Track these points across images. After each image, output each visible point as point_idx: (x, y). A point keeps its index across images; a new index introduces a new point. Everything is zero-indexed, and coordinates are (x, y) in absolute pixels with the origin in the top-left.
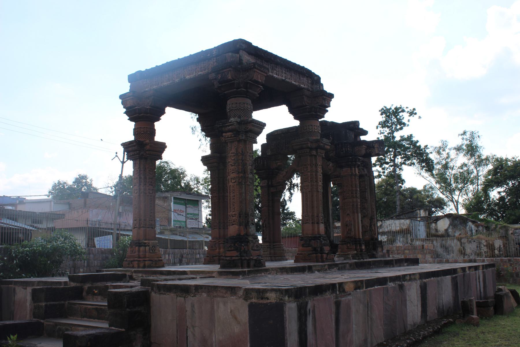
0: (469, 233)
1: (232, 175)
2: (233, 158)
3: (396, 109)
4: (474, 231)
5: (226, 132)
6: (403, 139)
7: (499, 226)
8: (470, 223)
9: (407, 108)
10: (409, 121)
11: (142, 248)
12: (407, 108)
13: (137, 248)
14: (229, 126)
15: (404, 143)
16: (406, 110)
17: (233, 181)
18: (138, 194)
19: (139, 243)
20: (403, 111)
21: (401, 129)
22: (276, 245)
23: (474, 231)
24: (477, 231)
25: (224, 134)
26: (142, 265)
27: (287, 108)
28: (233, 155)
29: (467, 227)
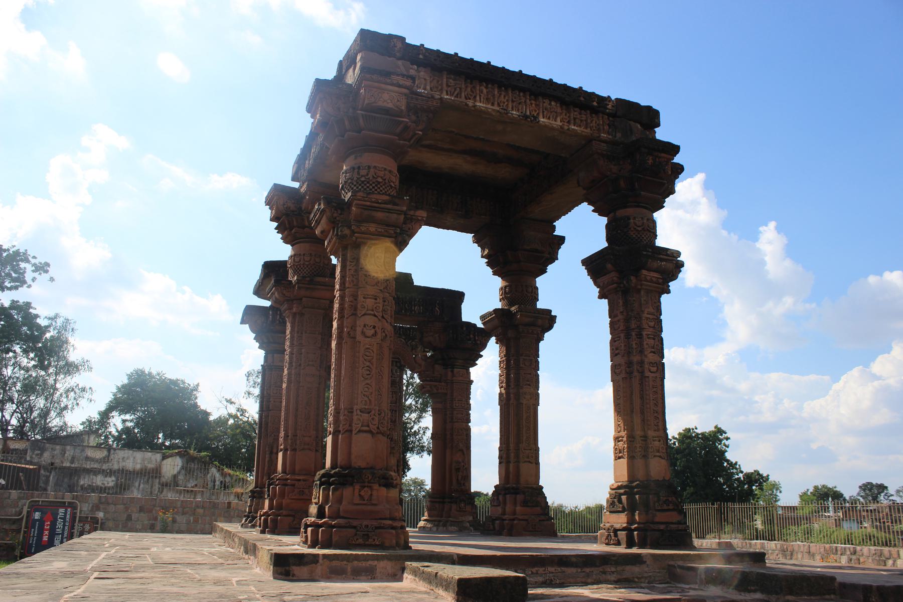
0: (210, 485)
3: (17, 253)
4: (218, 483)
5: (649, 270)
6: (14, 305)
8: (213, 470)
9: (34, 257)
10: (34, 280)
12: (34, 257)
13: (384, 490)
14: (662, 260)
15: (14, 312)
16: (33, 261)
20: (28, 261)
21: (16, 288)
23: (218, 483)
25: (644, 272)
27: (465, 240)
29: (209, 475)
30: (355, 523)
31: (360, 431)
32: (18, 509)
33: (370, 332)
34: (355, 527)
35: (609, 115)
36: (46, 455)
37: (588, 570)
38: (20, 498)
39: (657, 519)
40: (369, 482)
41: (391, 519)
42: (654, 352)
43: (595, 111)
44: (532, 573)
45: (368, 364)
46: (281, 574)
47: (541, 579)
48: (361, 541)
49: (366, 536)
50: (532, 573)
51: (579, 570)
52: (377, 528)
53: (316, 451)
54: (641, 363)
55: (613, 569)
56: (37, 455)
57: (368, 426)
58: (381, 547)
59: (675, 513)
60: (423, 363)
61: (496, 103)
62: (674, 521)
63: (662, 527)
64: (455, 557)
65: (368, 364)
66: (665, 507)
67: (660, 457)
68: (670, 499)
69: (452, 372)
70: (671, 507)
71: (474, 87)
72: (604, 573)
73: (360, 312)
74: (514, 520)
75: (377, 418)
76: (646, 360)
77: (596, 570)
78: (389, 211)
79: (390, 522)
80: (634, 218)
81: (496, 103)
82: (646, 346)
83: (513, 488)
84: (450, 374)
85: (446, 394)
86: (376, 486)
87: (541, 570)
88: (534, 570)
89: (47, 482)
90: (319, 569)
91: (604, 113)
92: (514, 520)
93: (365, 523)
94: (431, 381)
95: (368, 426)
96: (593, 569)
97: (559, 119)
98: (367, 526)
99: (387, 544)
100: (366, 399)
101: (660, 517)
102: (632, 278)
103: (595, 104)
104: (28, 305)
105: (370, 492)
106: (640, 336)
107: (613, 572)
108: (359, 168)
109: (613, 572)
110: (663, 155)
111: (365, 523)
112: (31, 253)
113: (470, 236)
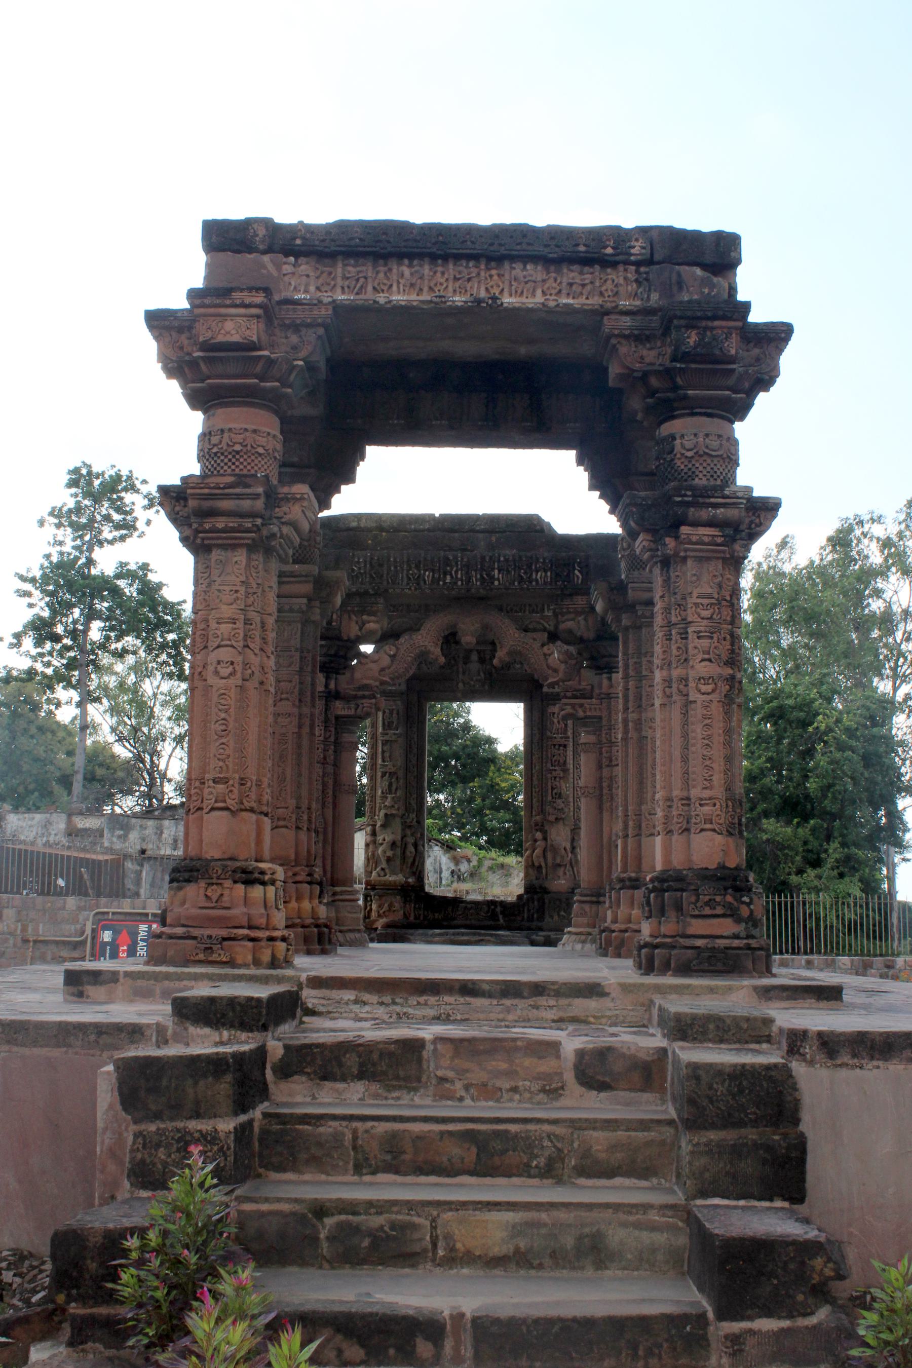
1: (703, 669)
2: (706, 613)
3: (117, 478)
5: (695, 524)
6: (124, 572)
7: (487, 863)
9: (144, 482)
10: (148, 523)
11: (257, 891)
12: (144, 482)
13: (241, 887)
14: (715, 506)
15: (122, 583)
17: (704, 688)
18: (237, 680)
19: (244, 871)
21: (123, 538)
22: (342, 893)
24: (453, 872)
25: (685, 530)
26: (266, 957)
28: (705, 601)
30: (195, 932)
31: (213, 809)
32: (78, 926)
33: (225, 672)
34: (195, 938)
35: (638, 264)
36: (133, 836)
37: (508, 1002)
38: (80, 909)
39: (691, 931)
40: (218, 878)
41: (250, 927)
42: (710, 660)
43: (607, 263)
44: (419, 1003)
45: (223, 715)
46: (73, 994)
47: (431, 1012)
48: (201, 956)
49: (209, 950)
50: (419, 1003)
51: (495, 1002)
52: (224, 939)
53: (298, 828)
54: (684, 680)
55: (552, 1002)
56: (119, 837)
57: (225, 801)
58: (231, 963)
59: (729, 921)
61: (426, 289)
62: (725, 934)
63: (699, 943)
64: (457, 986)
65: (223, 715)
66: (707, 911)
67: (714, 830)
68: (718, 898)
69: (610, 679)
70: (719, 910)
71: (390, 270)
72: (537, 1007)
73: (213, 643)
74: (626, 931)
75: (236, 791)
76: (692, 674)
77: (521, 1003)
78: (239, 497)
79: (245, 932)
80: (682, 436)
81: (426, 289)
82: (691, 651)
83: (630, 879)
84: (605, 682)
85: (600, 718)
86: (228, 883)
87: (432, 1000)
88: (422, 999)
89: (138, 882)
90: (120, 989)
91: (627, 263)
92: (626, 931)
93: (208, 932)
94: (576, 697)
95: (225, 801)
96: (516, 1001)
97: (539, 292)
98: (210, 937)
99: (239, 961)
100: (221, 764)
101: (697, 926)
102: (668, 540)
103: (609, 251)
104: (145, 567)
105: (219, 892)
106: (684, 636)
107: (551, 1007)
108: (210, 433)
109: (551, 1007)
110: (717, 323)
111: (208, 932)
112: (139, 475)
113: (571, 455)
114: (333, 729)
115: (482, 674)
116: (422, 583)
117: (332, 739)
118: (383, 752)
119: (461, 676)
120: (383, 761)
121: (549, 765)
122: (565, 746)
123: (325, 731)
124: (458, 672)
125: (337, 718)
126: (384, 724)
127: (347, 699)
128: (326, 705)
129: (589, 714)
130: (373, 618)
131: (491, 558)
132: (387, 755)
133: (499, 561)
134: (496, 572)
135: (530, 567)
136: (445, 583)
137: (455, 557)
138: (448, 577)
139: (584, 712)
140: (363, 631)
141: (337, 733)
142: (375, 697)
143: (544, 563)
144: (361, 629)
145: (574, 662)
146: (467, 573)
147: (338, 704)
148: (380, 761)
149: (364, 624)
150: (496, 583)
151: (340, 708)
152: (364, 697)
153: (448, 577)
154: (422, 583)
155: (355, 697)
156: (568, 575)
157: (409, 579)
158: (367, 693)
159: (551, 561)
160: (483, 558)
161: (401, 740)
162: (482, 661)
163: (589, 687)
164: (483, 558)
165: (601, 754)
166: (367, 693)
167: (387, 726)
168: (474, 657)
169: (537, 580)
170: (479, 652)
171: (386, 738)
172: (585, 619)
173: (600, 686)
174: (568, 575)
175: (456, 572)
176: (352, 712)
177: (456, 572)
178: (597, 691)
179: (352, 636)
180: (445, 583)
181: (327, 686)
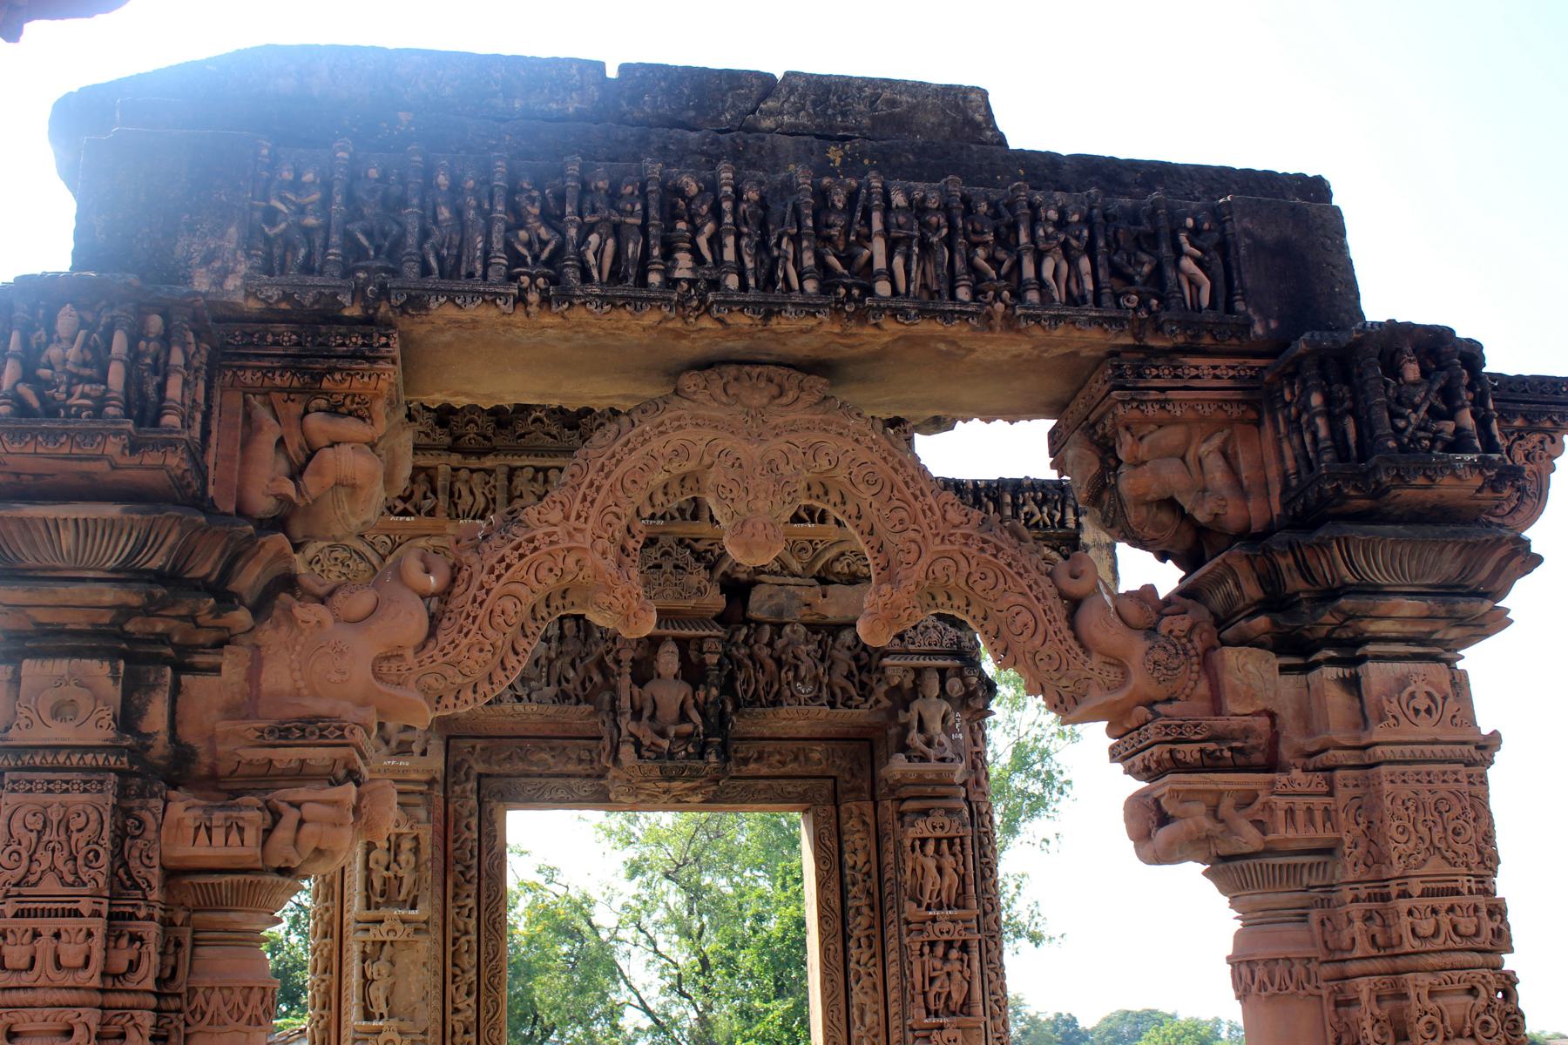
60: (1137, 649)
69: (1352, 685)
84: (1336, 698)
94: (1210, 764)
114: (152, 931)
115: (695, 716)
116: (572, 275)
117: (146, 977)
118: (367, 982)
119: (627, 725)
120: (368, 1016)
121: (918, 1015)
122: (965, 947)
123: (113, 936)
124: (614, 710)
125: (174, 874)
126: (368, 884)
127: (223, 787)
128: (122, 811)
129: (1282, 833)
130: (350, 427)
131: (852, 197)
132: (378, 993)
133: (887, 208)
134: (879, 247)
135: (1005, 238)
136: (670, 282)
137: (712, 187)
138: (684, 260)
139: (1258, 824)
140: (308, 479)
141: (170, 945)
142: (353, 776)
143: (1061, 224)
144: (296, 474)
145: (1181, 624)
146: (762, 246)
147: (183, 808)
148: (353, 1017)
149: (312, 452)
150: (883, 288)
151: (184, 830)
152: (301, 774)
153: (684, 260)
154: (572, 275)
155: (266, 778)
156: (1158, 271)
157: (516, 259)
158: (319, 756)
159: (1087, 220)
160: (822, 195)
161: (426, 946)
162: (692, 672)
163: (1262, 723)
164: (822, 195)
165: (1344, 1003)
166: (319, 756)
167: (380, 894)
168: (668, 661)
169: (1042, 285)
170: (682, 643)
171: (377, 933)
172: (1224, 453)
173: (1305, 717)
174: (1158, 273)
175: (716, 242)
176: (247, 849)
177: (716, 242)
178: (1293, 740)
179: (263, 504)
180: (670, 282)
181: (127, 719)
